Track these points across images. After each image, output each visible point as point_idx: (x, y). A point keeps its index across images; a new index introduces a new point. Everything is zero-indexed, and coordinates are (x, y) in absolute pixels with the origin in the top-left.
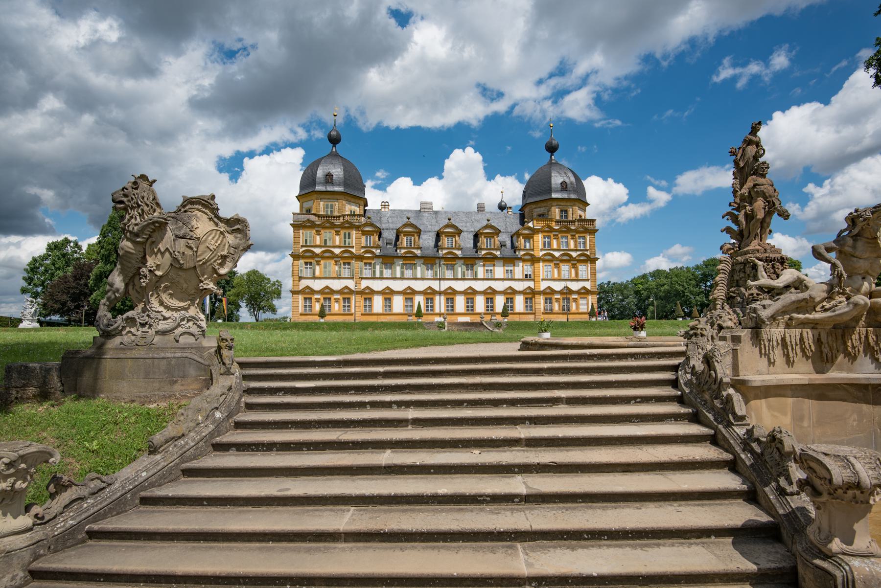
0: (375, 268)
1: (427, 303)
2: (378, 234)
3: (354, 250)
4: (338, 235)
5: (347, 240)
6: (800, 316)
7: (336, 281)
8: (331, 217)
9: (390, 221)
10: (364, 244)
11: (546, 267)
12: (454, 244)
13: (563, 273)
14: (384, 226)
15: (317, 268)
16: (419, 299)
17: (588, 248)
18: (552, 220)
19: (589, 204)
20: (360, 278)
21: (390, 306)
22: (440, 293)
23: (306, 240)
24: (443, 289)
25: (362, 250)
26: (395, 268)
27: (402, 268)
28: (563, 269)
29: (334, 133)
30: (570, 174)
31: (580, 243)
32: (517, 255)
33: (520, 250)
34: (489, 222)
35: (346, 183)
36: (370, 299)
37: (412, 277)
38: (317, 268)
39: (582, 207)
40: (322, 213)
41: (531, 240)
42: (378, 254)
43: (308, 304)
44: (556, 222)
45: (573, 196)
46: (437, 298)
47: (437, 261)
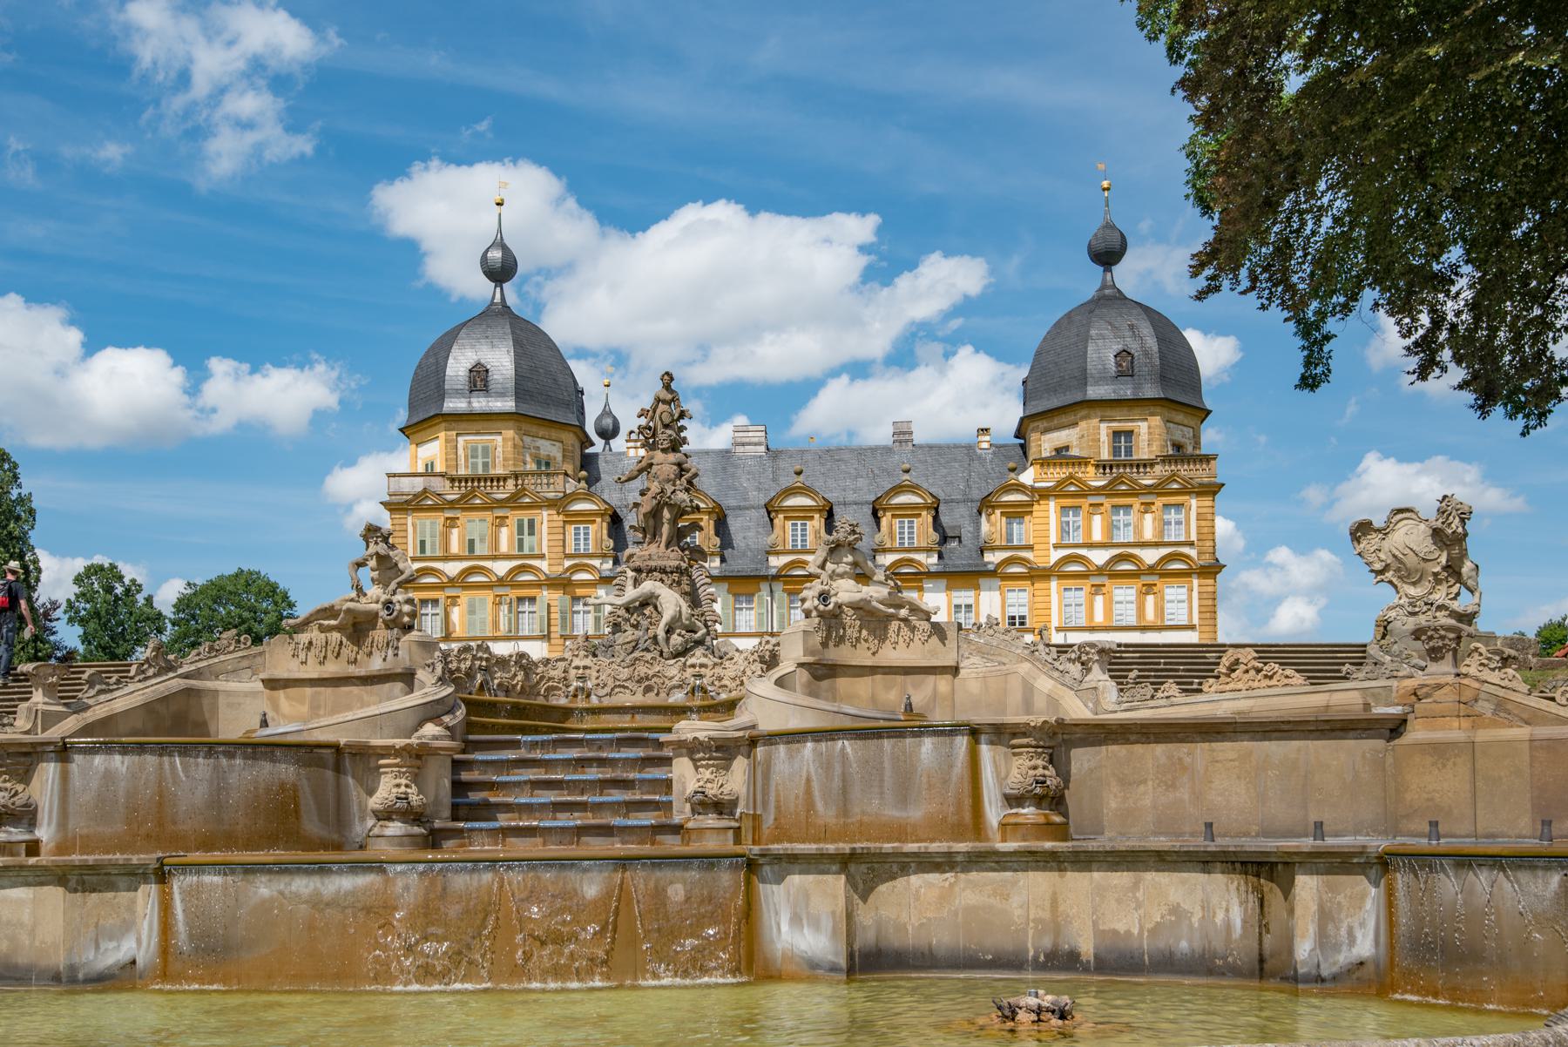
2: (608, 519)
3: (543, 565)
5: (526, 537)
6: (326, 622)
8: (485, 480)
10: (570, 549)
11: (1068, 594)
12: (810, 538)
13: (1117, 609)
17: (1194, 537)
18: (1082, 462)
19: (1208, 412)
20: (562, 636)
23: (423, 543)
25: (568, 563)
28: (1116, 599)
30: (1146, 330)
31: (1169, 523)
32: (989, 563)
33: (993, 549)
34: (906, 477)
38: (456, 614)
39: (1186, 422)
40: (462, 472)
41: (1027, 518)
42: (607, 574)
44: (1097, 466)
45: (1150, 391)
47: (764, 587)
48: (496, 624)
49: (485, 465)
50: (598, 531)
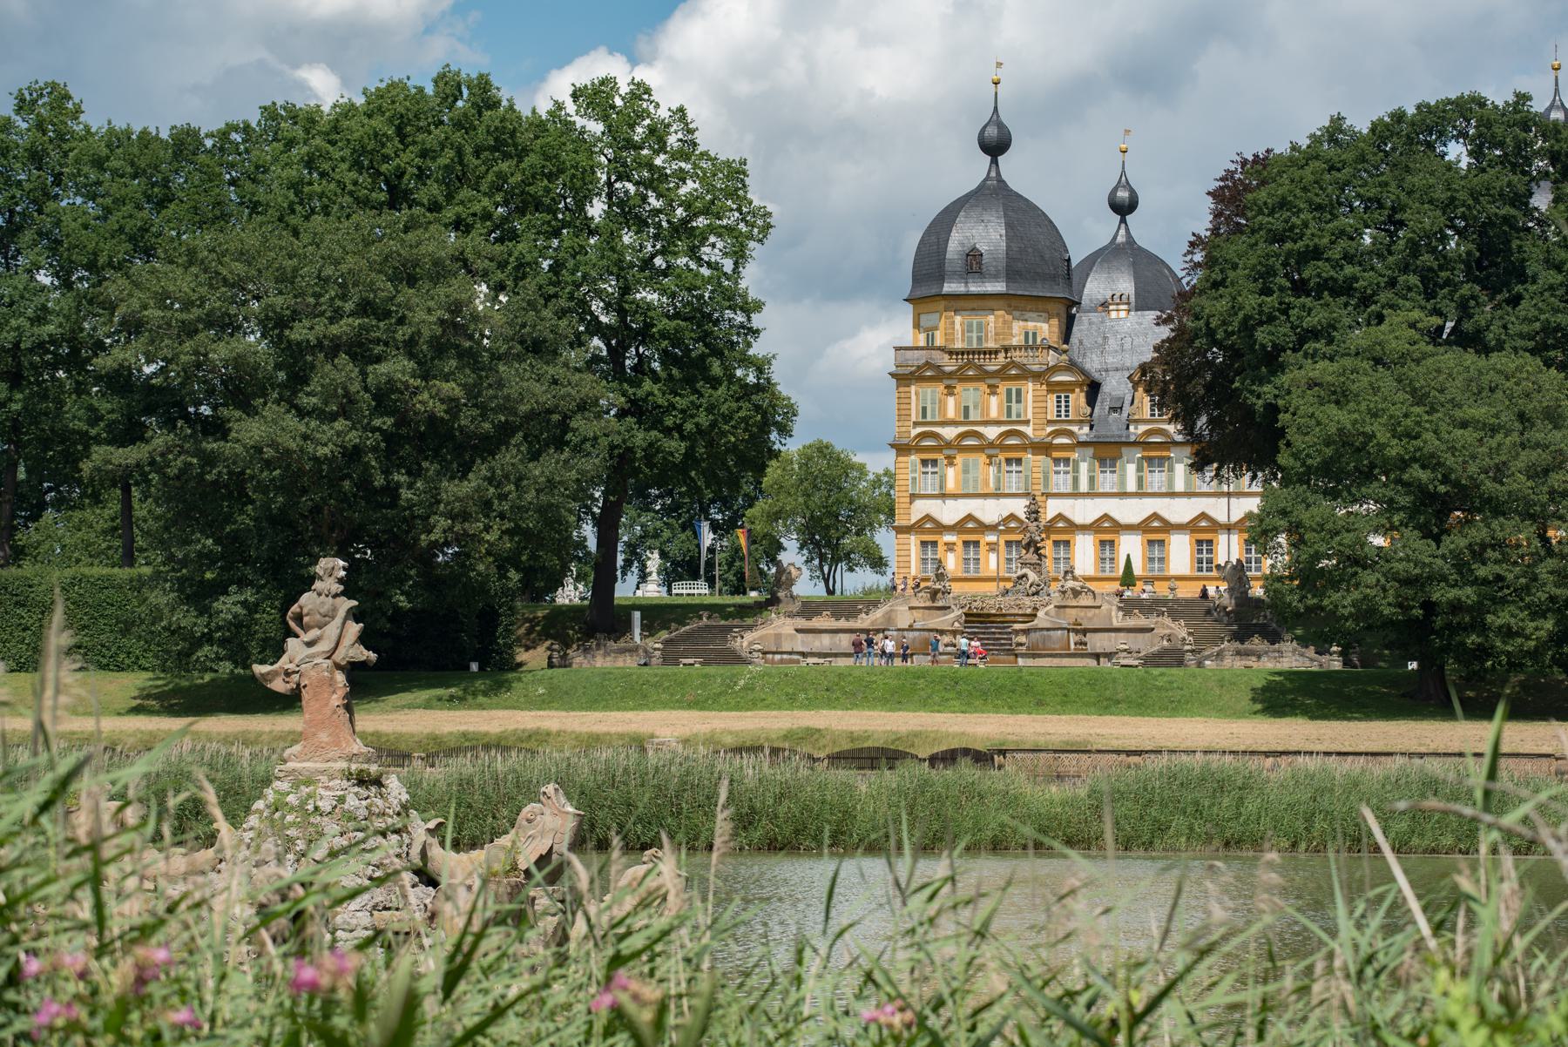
0: (1076, 470)
1: (1200, 551)
3: (1028, 430)
4: (994, 393)
5: (1014, 405)
7: (991, 502)
9: (1127, 346)
10: (1052, 415)
14: (1110, 360)
15: (951, 472)
16: (1131, 547)
21: (1112, 559)
22: (1229, 528)
23: (924, 409)
24: (1234, 519)
25: (1049, 429)
26: (1124, 469)
27: (1139, 469)
29: (992, 132)
35: (1012, 273)
36: (1067, 543)
37: (1164, 490)
38: (951, 472)
40: (959, 345)
42: (1083, 438)
43: (930, 555)
46: (1222, 539)
48: (986, 483)
49: (979, 339)
50: (1078, 398)
